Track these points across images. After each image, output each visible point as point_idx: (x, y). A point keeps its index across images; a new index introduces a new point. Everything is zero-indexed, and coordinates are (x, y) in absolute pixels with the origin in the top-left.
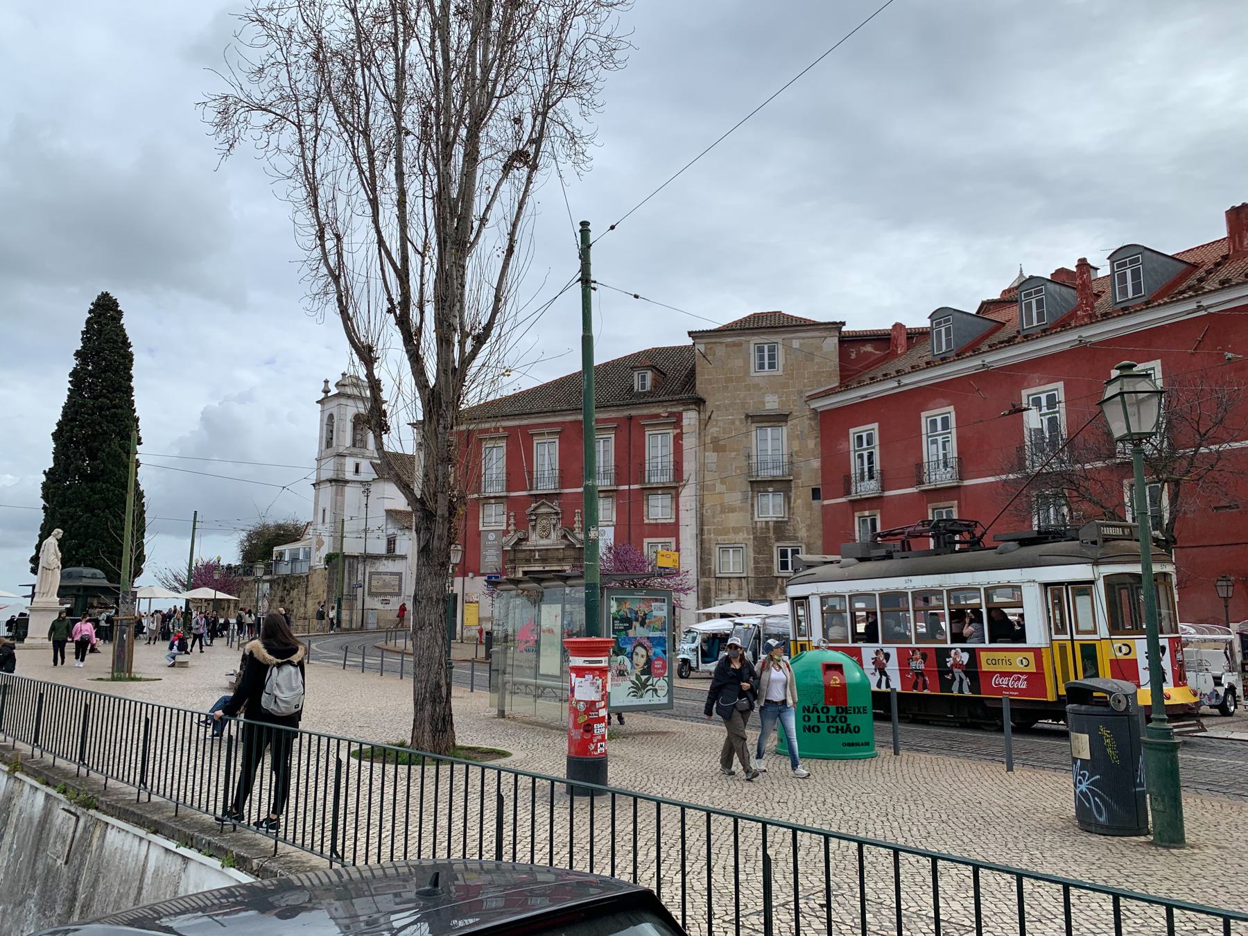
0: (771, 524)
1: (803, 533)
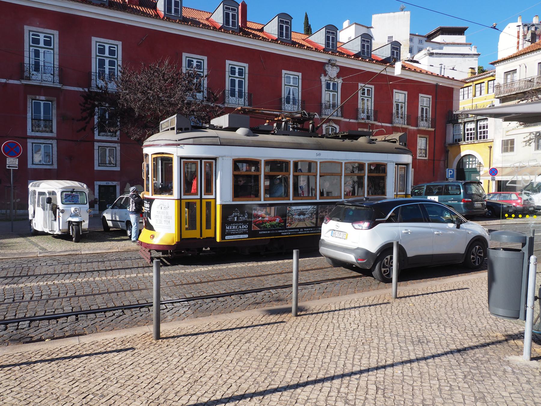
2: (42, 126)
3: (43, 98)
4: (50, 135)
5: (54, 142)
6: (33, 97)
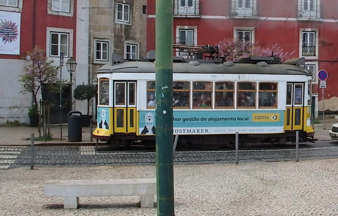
0: (123, 27)
1: (138, 36)
2: (309, 51)
3: (309, 30)
4: (314, 58)
5: (316, 63)
6: (303, 29)
